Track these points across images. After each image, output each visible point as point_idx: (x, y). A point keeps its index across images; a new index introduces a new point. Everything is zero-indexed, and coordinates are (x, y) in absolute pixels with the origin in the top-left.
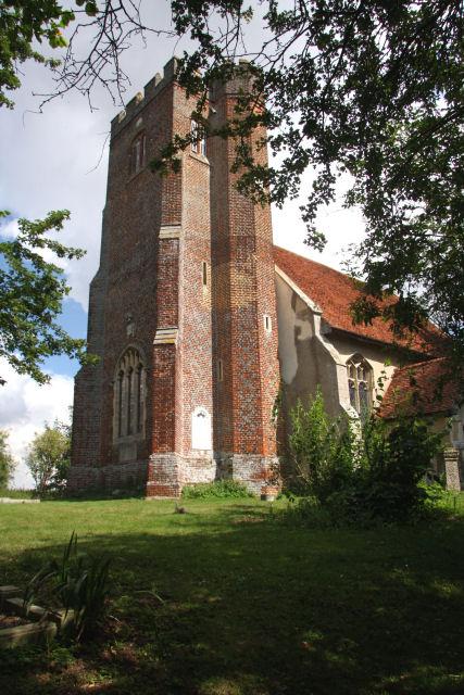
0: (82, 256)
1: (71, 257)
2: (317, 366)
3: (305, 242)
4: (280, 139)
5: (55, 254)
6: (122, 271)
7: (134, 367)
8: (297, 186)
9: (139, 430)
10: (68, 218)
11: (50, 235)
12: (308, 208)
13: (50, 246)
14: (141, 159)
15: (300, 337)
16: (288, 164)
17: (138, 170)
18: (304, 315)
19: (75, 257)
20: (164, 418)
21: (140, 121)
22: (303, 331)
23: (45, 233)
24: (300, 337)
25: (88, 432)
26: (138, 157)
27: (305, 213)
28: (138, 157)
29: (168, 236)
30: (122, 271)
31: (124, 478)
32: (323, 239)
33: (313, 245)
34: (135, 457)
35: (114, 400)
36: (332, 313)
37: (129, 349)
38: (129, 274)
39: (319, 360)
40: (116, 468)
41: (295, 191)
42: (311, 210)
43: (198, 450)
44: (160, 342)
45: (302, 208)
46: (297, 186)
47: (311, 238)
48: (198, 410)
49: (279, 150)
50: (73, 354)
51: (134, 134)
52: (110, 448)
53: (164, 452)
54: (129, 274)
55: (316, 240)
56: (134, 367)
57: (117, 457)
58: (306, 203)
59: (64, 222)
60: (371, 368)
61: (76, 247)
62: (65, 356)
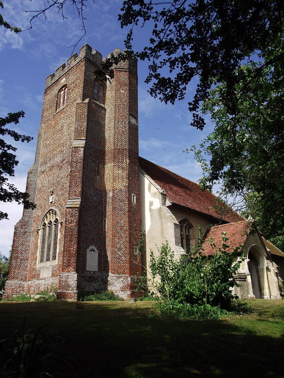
0: (29, 140)
1: (23, 141)
2: (162, 224)
3: (192, 124)
4: (176, 59)
5: (13, 138)
6: (49, 165)
7: (53, 221)
8: (184, 92)
9: (54, 258)
10: (23, 116)
11: (8, 126)
12: (193, 103)
13: (9, 133)
14: (64, 101)
15: (152, 207)
16: (179, 77)
17: (61, 108)
18: (155, 195)
19: (26, 141)
20: (70, 251)
21: (64, 79)
22: (154, 204)
23: (6, 125)
24: (152, 207)
25: (21, 260)
26: (62, 100)
27: (191, 106)
28: (62, 100)
29: (78, 146)
30: (49, 165)
31: (42, 289)
32: (203, 122)
33: (196, 126)
34: (50, 275)
35: (39, 241)
36: (171, 194)
37: (51, 210)
38: (53, 167)
39: (164, 221)
40: (37, 282)
41: (182, 94)
42: (195, 105)
43: (90, 272)
44: (78, 200)
45: (190, 104)
46: (184, 92)
47: (195, 121)
48: (91, 248)
49: (174, 69)
50: (21, 201)
51: (60, 87)
52: (34, 269)
53: (69, 272)
54: (53, 167)
55: (198, 123)
56: (53, 221)
57: (39, 275)
58: (192, 99)
59: (20, 119)
60: (193, 227)
61: (27, 135)
62: (14, 201)
